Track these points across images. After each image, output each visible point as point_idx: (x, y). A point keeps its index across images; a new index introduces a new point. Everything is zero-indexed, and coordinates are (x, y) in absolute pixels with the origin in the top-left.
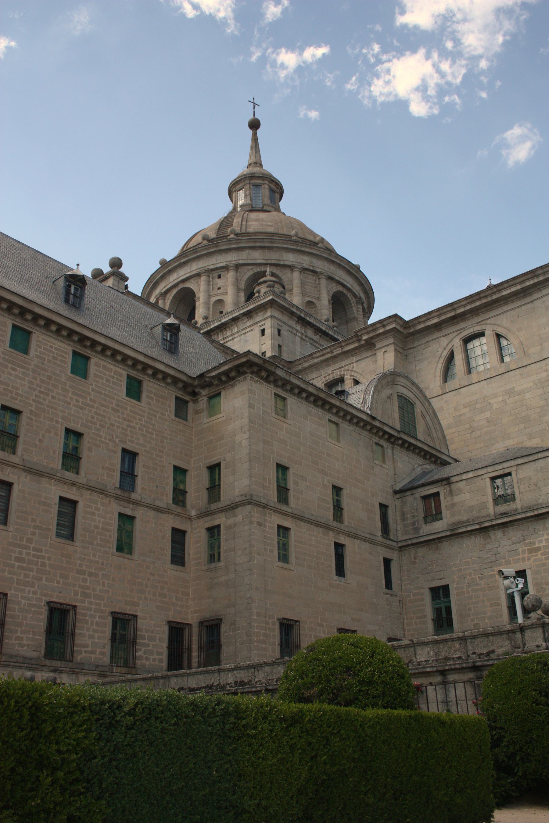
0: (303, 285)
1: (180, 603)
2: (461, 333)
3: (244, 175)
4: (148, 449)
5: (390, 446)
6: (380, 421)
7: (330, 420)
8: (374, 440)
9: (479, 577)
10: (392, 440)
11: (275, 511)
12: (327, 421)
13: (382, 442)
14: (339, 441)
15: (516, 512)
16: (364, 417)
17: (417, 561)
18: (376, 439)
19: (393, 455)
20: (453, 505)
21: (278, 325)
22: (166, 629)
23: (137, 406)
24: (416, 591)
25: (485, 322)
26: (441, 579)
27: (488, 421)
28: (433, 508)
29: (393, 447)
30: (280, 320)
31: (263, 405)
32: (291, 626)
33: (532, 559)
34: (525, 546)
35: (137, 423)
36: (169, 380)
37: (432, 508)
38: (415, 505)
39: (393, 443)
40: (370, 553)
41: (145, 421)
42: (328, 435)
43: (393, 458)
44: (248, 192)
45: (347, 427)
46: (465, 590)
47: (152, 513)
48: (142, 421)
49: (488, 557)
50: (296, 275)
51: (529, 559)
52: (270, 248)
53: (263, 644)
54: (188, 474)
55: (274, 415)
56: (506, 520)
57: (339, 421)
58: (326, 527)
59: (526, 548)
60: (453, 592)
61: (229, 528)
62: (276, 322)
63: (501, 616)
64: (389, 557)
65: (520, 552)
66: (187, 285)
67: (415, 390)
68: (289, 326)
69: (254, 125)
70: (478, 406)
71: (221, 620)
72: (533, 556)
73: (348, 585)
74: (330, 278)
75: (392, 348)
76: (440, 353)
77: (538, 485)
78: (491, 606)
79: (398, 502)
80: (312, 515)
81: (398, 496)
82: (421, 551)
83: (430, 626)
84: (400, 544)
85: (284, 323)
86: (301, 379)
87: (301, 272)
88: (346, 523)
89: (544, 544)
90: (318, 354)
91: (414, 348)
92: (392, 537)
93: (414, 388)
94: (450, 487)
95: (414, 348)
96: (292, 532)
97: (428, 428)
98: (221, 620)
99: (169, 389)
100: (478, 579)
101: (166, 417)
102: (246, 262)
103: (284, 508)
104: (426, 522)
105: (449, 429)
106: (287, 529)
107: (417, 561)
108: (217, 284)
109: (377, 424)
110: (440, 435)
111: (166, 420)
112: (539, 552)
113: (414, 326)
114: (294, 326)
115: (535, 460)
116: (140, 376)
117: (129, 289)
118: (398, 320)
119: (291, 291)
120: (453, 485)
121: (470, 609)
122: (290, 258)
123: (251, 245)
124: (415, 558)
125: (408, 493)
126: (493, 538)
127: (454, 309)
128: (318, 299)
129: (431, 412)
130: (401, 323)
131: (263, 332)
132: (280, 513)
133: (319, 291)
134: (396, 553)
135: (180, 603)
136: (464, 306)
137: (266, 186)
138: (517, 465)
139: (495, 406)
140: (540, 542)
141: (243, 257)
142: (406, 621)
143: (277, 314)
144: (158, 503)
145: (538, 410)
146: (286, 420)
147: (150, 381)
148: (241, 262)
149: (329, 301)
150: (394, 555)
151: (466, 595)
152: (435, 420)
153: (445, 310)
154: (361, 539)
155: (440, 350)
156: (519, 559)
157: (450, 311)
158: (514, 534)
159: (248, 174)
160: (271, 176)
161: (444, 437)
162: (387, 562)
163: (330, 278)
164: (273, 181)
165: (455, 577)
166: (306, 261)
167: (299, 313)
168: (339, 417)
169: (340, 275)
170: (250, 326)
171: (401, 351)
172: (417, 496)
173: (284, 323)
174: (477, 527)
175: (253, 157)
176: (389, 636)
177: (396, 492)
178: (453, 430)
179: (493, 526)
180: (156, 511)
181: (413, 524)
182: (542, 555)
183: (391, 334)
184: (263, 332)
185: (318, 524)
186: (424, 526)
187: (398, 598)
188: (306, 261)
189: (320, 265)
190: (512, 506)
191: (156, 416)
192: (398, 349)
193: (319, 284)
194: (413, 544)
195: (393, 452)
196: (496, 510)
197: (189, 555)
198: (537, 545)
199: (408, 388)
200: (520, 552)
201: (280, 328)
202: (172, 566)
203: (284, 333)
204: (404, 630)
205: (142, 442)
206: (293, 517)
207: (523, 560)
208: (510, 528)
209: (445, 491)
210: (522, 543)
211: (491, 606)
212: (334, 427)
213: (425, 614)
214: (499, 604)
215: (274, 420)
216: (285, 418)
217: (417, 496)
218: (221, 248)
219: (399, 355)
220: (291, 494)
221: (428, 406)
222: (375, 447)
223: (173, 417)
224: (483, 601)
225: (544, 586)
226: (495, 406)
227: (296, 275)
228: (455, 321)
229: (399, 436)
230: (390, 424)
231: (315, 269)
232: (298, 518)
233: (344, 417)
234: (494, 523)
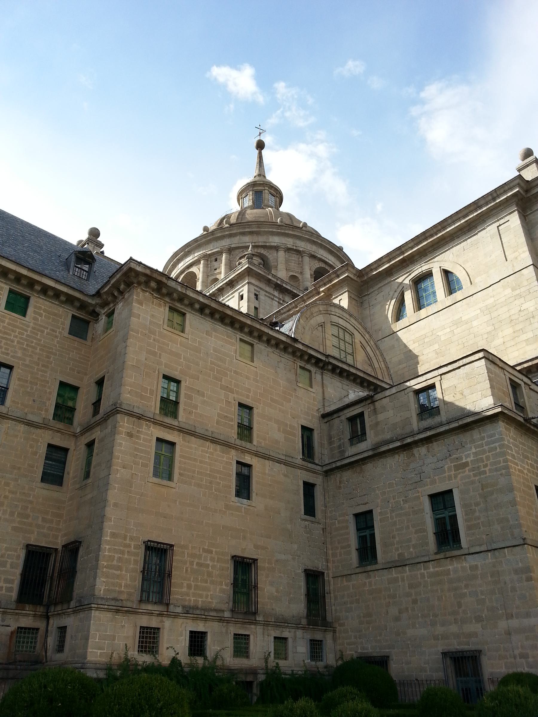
0: (287, 261)
1: (47, 525)
2: (410, 274)
3: (248, 184)
4: (27, 362)
5: (319, 371)
6: (303, 344)
7: (241, 340)
8: (299, 364)
9: (403, 500)
10: (321, 365)
11: (154, 423)
12: (238, 340)
13: (308, 367)
14: (252, 361)
15: (441, 425)
16: (283, 339)
17: (342, 485)
18: (300, 363)
19: (323, 380)
20: (377, 424)
21: (255, 290)
22: (22, 554)
23: (19, 320)
24: (340, 518)
25: (432, 261)
26: (365, 504)
27: (437, 353)
28: (359, 430)
29: (322, 373)
30: (257, 286)
31: (153, 316)
32: (166, 550)
33: (459, 476)
34: (451, 463)
35: (16, 337)
36: (63, 298)
37: (357, 426)
38: (341, 427)
39: (322, 368)
40: (285, 476)
41: (27, 335)
42: (238, 353)
43: (323, 383)
44: (251, 198)
45: (263, 348)
46: (389, 515)
47: (22, 428)
48: (23, 334)
49: (412, 477)
50: (281, 254)
51: (456, 477)
52: (258, 233)
53: (117, 570)
54: (80, 391)
55: (165, 327)
56: (429, 433)
57: (255, 341)
58: (227, 445)
59: (452, 464)
60: (377, 518)
61: (102, 440)
62: (253, 288)
63: (427, 544)
64: (311, 481)
65: (446, 469)
66: (191, 270)
67: (354, 321)
68: (266, 292)
69: (260, 146)
70: (426, 340)
71: (80, 542)
72: (459, 473)
73: (251, 508)
74: (313, 257)
75: (346, 294)
76: (391, 295)
77: (464, 394)
78: (416, 532)
79: (325, 427)
80: (207, 430)
81: (326, 420)
82: (347, 475)
83: (354, 556)
84: (325, 469)
85: (261, 288)
86: (215, 300)
87: (285, 252)
88: (255, 443)
89: (472, 458)
90: (285, 310)
91: (368, 295)
92: (317, 461)
93: (352, 319)
94: (374, 406)
95: (368, 295)
96: (178, 447)
97: (369, 359)
98: (80, 542)
99: (64, 307)
100: (402, 502)
101: (57, 334)
103: (169, 420)
104: (352, 444)
105: (400, 364)
106: (172, 444)
107: (342, 485)
108: (214, 266)
109: (301, 347)
110: (383, 366)
111: (56, 337)
112: (467, 468)
113: (367, 274)
114: (272, 292)
115: (459, 367)
116: (26, 292)
117: (105, 255)
118: (350, 268)
119: (276, 267)
120: (377, 404)
121: (394, 537)
122: (275, 240)
123: (241, 230)
124: (340, 482)
125: (335, 416)
126: (417, 456)
127: (403, 253)
128: (301, 273)
129: (373, 344)
130: (354, 272)
131: (242, 297)
132: (161, 425)
133: (302, 267)
134: (321, 477)
135: (47, 525)
136: (412, 248)
137: (266, 191)
138: (441, 375)
139: (443, 338)
140: (468, 456)
141: (235, 242)
142: (330, 552)
143: (253, 281)
144: (30, 417)
145: (486, 336)
146: (182, 334)
147: (39, 297)
149: (311, 275)
150: (317, 480)
151: (390, 521)
152: (377, 352)
153: (394, 255)
154: (273, 460)
155: (391, 293)
156: (445, 477)
157: (399, 255)
158: (439, 448)
159: (251, 182)
160: (271, 183)
161: (387, 368)
162: (309, 488)
163: (313, 257)
164: (272, 187)
165: (379, 501)
166: (289, 242)
167: (275, 280)
168: (254, 337)
169: (322, 253)
170: (232, 294)
171: (356, 298)
172: (343, 418)
173: (261, 288)
174: (398, 444)
175: (257, 171)
176: (306, 568)
177: (324, 416)
178: (404, 365)
179: (416, 443)
180: (27, 425)
181: (339, 447)
182: (469, 471)
183: (345, 283)
184: (242, 297)
185: (214, 441)
186: (349, 449)
187: (321, 526)
188: (289, 242)
189: (302, 245)
190: (437, 420)
191: (43, 332)
192: (353, 296)
193: (302, 261)
194: (337, 468)
195: (322, 378)
196: (420, 424)
197: (68, 474)
198: (464, 461)
199: (345, 319)
200: (446, 469)
201: (257, 293)
202: (43, 485)
203: (262, 297)
204: (327, 561)
205: (19, 355)
206: (179, 431)
207: (450, 478)
208: (435, 443)
209: (369, 410)
210: (448, 460)
211: (416, 532)
212: (248, 348)
213: (349, 543)
214: (425, 530)
215: (165, 332)
216: (182, 332)
217: (343, 418)
218: (217, 236)
219: (354, 302)
220: (181, 407)
221: (369, 338)
222: (299, 371)
223: (66, 333)
224: (408, 527)
225: (474, 507)
226: (443, 338)
227: (281, 254)
228: (405, 264)
229: (327, 361)
230: (321, 351)
231: (298, 248)
232: (188, 432)
233: (260, 338)
234: (416, 438)
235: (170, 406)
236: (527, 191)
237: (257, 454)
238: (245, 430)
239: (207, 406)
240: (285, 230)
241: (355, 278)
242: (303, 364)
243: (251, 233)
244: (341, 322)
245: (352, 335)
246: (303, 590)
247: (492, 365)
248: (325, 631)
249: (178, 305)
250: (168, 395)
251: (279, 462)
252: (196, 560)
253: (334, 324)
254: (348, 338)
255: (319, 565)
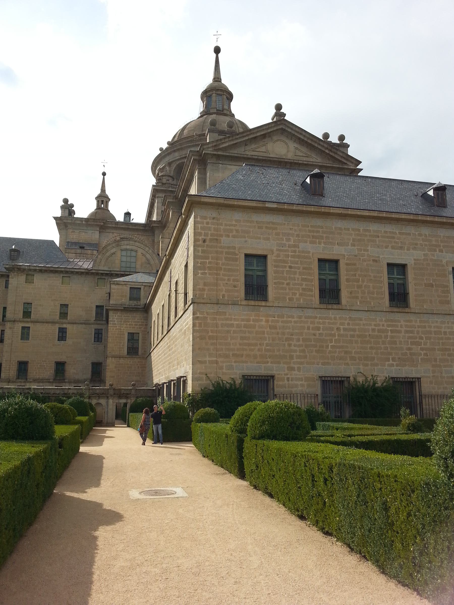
13: (104, 277)
18: (97, 277)
52: (182, 149)
55: (25, 284)
58: (53, 323)
69: (217, 50)
102: (172, 160)
109: (94, 271)
123: (172, 150)
148: (170, 161)
212: (68, 278)
235: (27, 314)
236: (201, 155)
237: (69, 323)
238: (64, 314)
239: (46, 308)
240: (196, 142)
241: (174, 201)
242: (100, 277)
243: (178, 150)
244: (128, 247)
245: (136, 251)
246: (90, 370)
247: (117, 285)
248: (101, 383)
249: (30, 273)
250: (28, 310)
251: (81, 324)
252: (39, 365)
253: (122, 250)
254: (133, 254)
255: (100, 360)
